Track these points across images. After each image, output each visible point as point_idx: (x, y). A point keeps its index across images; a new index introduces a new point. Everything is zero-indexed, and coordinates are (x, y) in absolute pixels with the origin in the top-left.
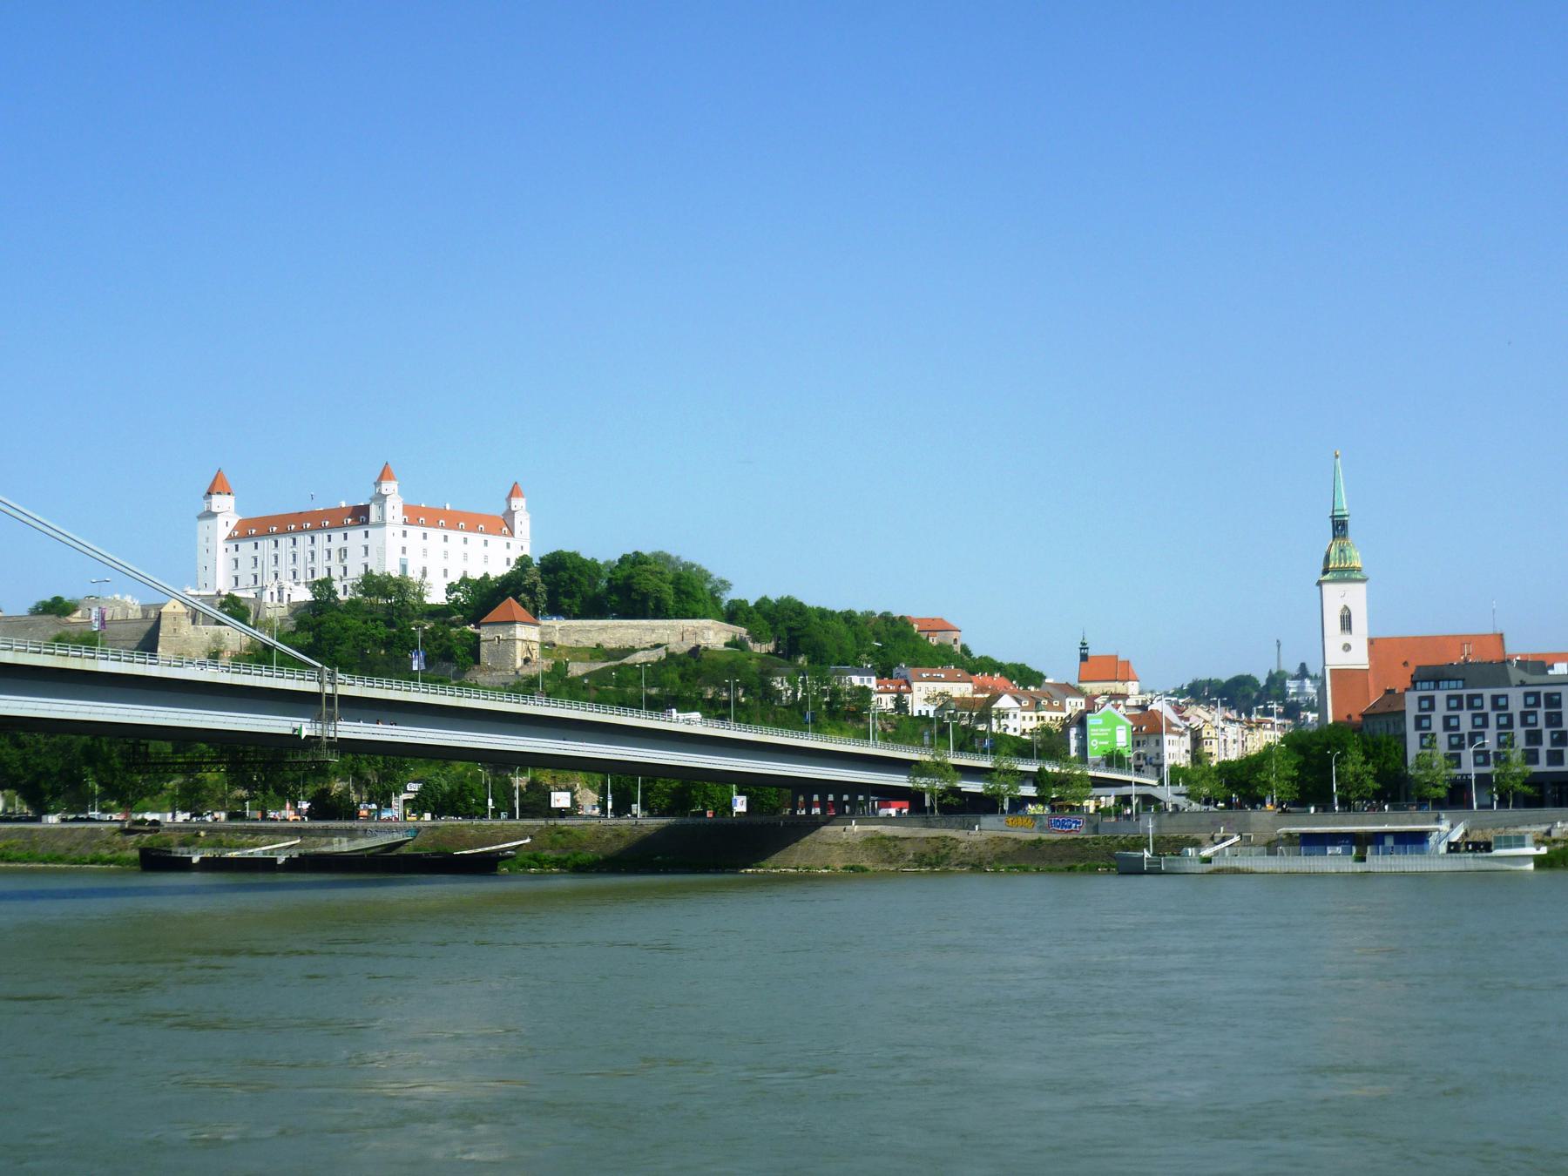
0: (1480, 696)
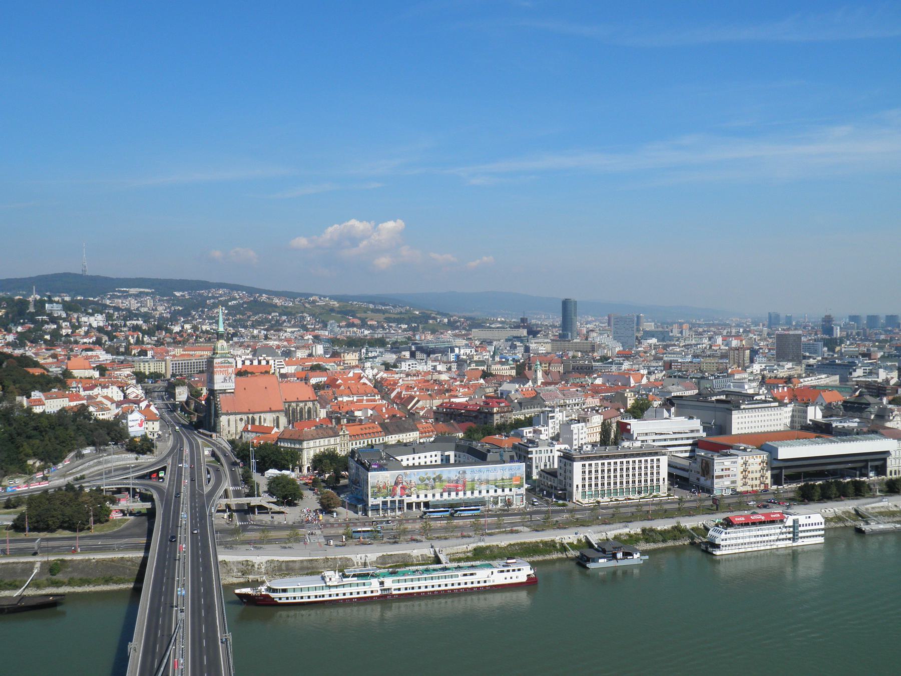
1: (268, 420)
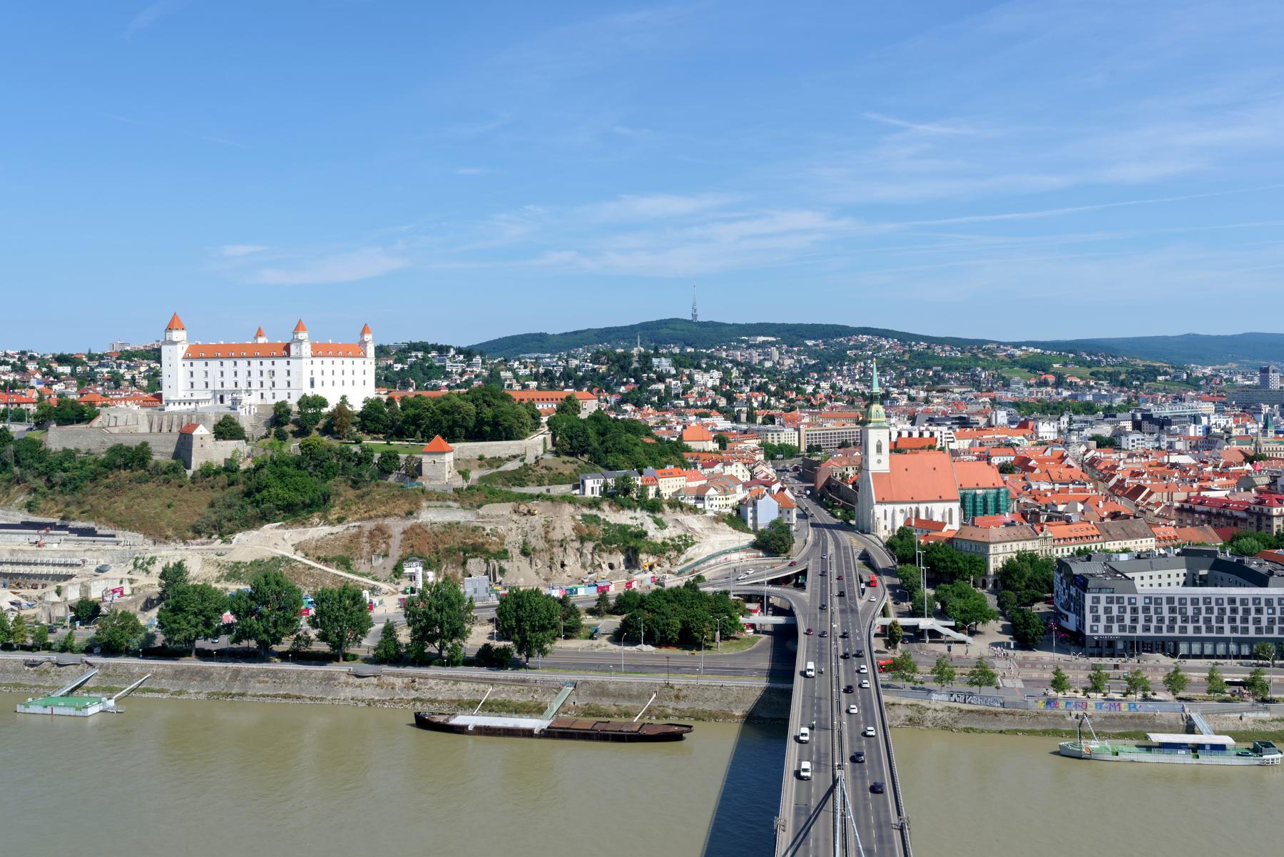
0: (1123, 598)
1: (937, 511)
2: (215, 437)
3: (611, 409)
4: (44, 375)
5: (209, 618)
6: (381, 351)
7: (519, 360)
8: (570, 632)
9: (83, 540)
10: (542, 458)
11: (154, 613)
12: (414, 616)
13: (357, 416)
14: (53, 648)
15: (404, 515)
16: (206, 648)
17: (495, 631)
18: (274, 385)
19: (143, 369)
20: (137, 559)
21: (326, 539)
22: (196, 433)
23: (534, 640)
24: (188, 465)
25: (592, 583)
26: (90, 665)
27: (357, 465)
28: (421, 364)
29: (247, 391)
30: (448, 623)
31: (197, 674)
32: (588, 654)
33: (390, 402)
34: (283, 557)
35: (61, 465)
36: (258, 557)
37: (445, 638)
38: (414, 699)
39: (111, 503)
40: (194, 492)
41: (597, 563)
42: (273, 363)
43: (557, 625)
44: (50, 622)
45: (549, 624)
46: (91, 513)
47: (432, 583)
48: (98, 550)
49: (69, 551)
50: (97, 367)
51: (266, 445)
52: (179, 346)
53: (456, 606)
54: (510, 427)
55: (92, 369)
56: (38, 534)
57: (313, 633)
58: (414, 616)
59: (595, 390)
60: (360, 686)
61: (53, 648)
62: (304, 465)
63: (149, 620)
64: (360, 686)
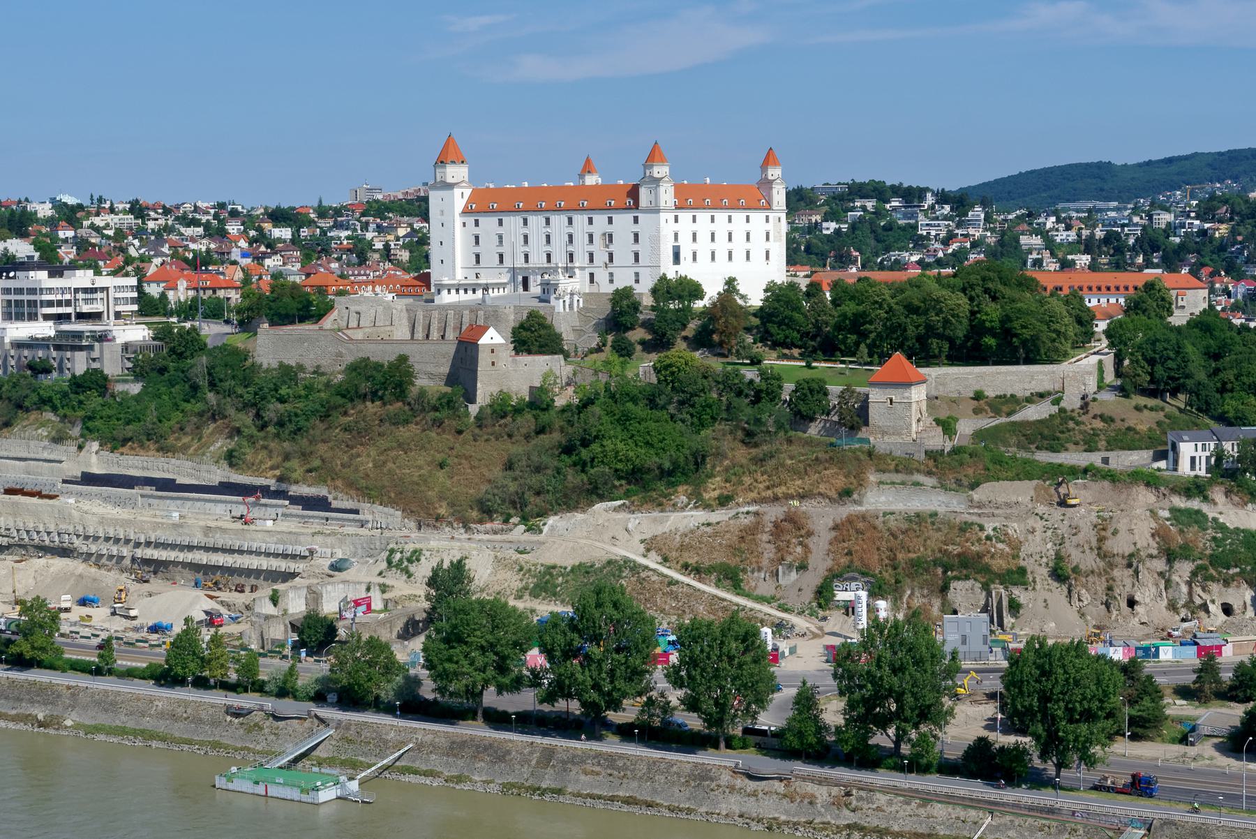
2: (515, 348)
3: (1235, 308)
4: (251, 242)
5: (504, 658)
6: (798, 199)
7: (1056, 213)
8: (1142, 728)
9: (313, 517)
10: (1094, 400)
11: (417, 643)
12: (851, 678)
13: (755, 315)
14: (267, 689)
15: (834, 495)
16: (501, 708)
17: (1000, 716)
18: (611, 260)
19: (402, 232)
20: (392, 551)
21: (700, 532)
22: (485, 340)
23: (1071, 737)
24: (471, 398)
25: (1189, 637)
26: (322, 721)
27: (753, 403)
28: (872, 223)
29: (566, 269)
30: (913, 694)
31: (486, 749)
32: (1176, 771)
33: (814, 290)
34: (627, 561)
35: (276, 391)
36: (585, 559)
37: (906, 720)
38: (848, 826)
39: (352, 457)
40: (481, 443)
41: (1198, 601)
42: (610, 221)
43: (1118, 714)
44: (263, 648)
45: (1101, 708)
46: (323, 473)
47: (886, 620)
48: (333, 534)
49: (290, 533)
50: (331, 229)
51: (599, 363)
52: (457, 191)
53: (928, 666)
54: (1035, 339)
55: (324, 233)
56: (245, 503)
57: (675, 696)
58: (851, 678)
59: (1204, 272)
60: (754, 794)
61: (267, 689)
62: (661, 401)
63: (410, 653)
64: (754, 794)
